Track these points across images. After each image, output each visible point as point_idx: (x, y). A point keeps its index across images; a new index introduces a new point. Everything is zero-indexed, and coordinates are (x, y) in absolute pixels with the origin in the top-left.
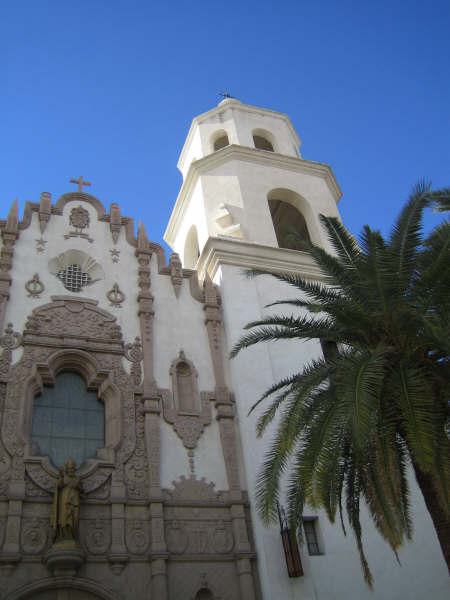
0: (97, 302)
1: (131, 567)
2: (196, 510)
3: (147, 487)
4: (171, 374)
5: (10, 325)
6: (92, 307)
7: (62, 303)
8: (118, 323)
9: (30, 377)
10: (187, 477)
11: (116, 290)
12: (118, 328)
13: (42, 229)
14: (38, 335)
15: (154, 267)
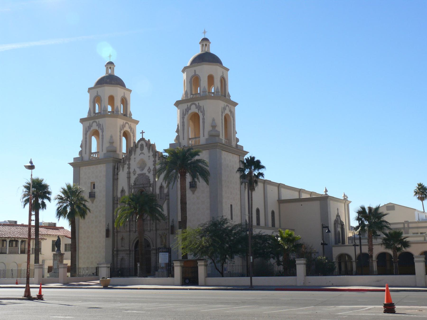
0: (146, 173)
5: (131, 184)
11: (149, 168)
12: (149, 180)
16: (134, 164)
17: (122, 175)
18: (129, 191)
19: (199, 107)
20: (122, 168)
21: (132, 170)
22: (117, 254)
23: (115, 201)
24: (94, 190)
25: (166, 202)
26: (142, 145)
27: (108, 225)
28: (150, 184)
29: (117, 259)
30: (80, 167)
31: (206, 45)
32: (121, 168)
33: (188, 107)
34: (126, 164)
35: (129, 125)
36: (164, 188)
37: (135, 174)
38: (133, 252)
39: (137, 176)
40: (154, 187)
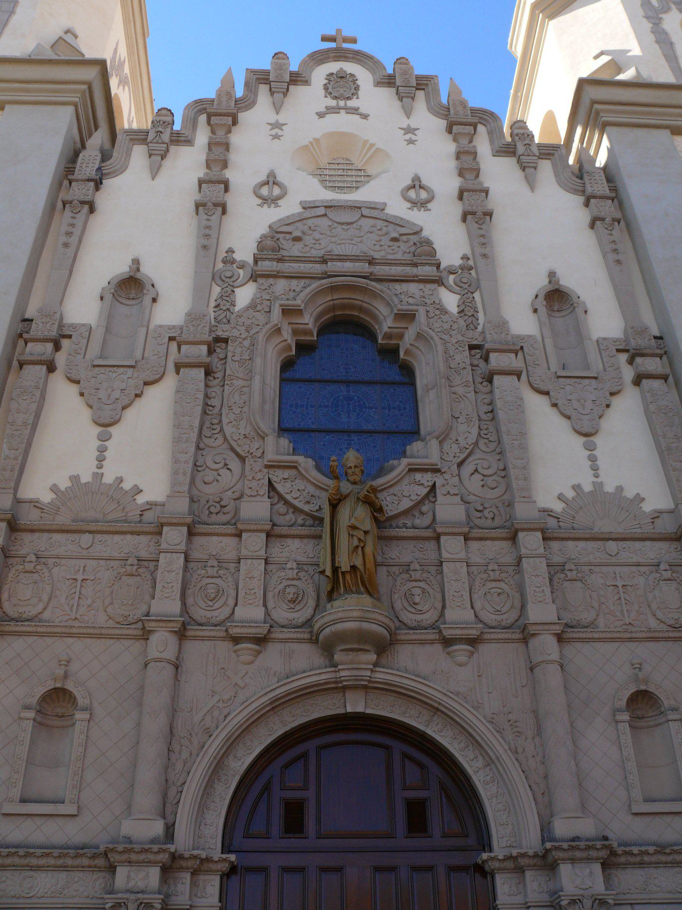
1: (483, 648)
2: (612, 546)
3: (510, 505)
4: (535, 311)
5: (231, 251)
6: (375, 213)
7: (322, 211)
8: (425, 233)
9: (268, 326)
10: (587, 488)
11: (417, 184)
13: (277, 109)
14: (280, 260)
15: (483, 145)
18: (199, 292)
34: (189, 142)
39: (301, 213)
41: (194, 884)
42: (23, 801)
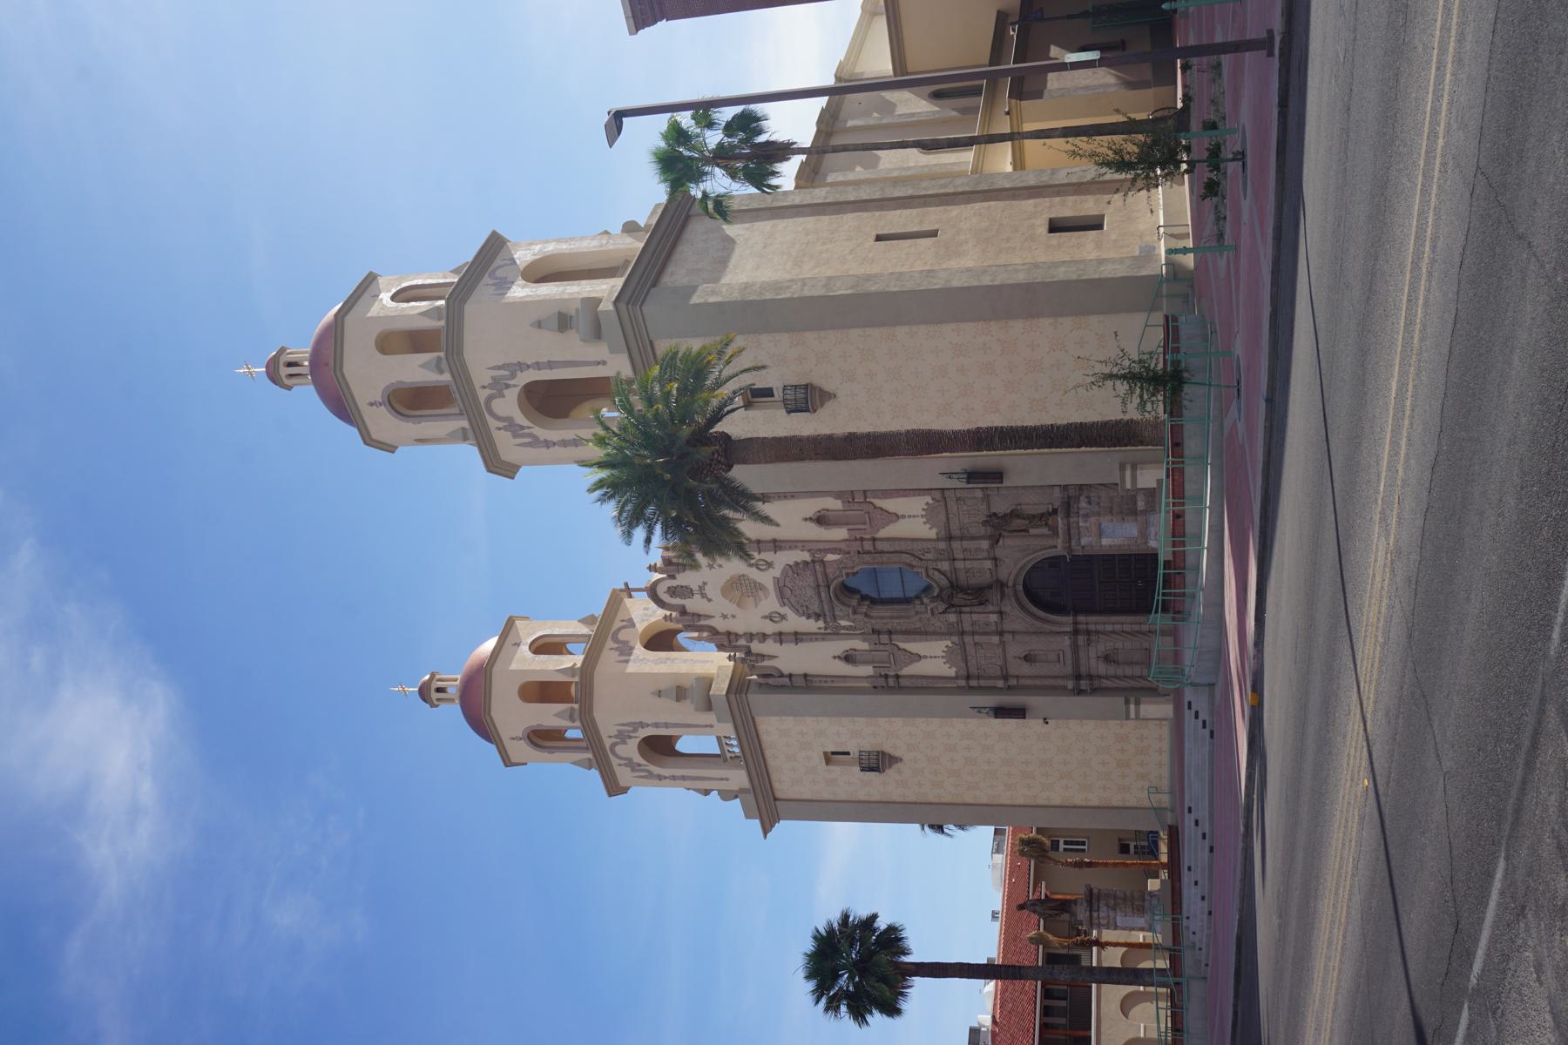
0: (774, 578)
5: (820, 628)
7: (786, 601)
12: (797, 564)
16: (748, 619)
17: (790, 659)
18: (848, 636)
19: (499, 386)
20: (763, 660)
21: (769, 628)
22: (1090, 677)
23: (890, 684)
24: (854, 751)
25: (878, 502)
26: (673, 592)
27: (979, 709)
28: (813, 561)
29: (1107, 678)
30: (776, 799)
31: (290, 364)
32: (766, 663)
33: (505, 428)
34: (749, 647)
35: (624, 627)
36: (823, 510)
37: (783, 617)
38: (1081, 618)
39: (789, 607)
40: (822, 546)
41: (1080, 624)
42: (1059, 661)
